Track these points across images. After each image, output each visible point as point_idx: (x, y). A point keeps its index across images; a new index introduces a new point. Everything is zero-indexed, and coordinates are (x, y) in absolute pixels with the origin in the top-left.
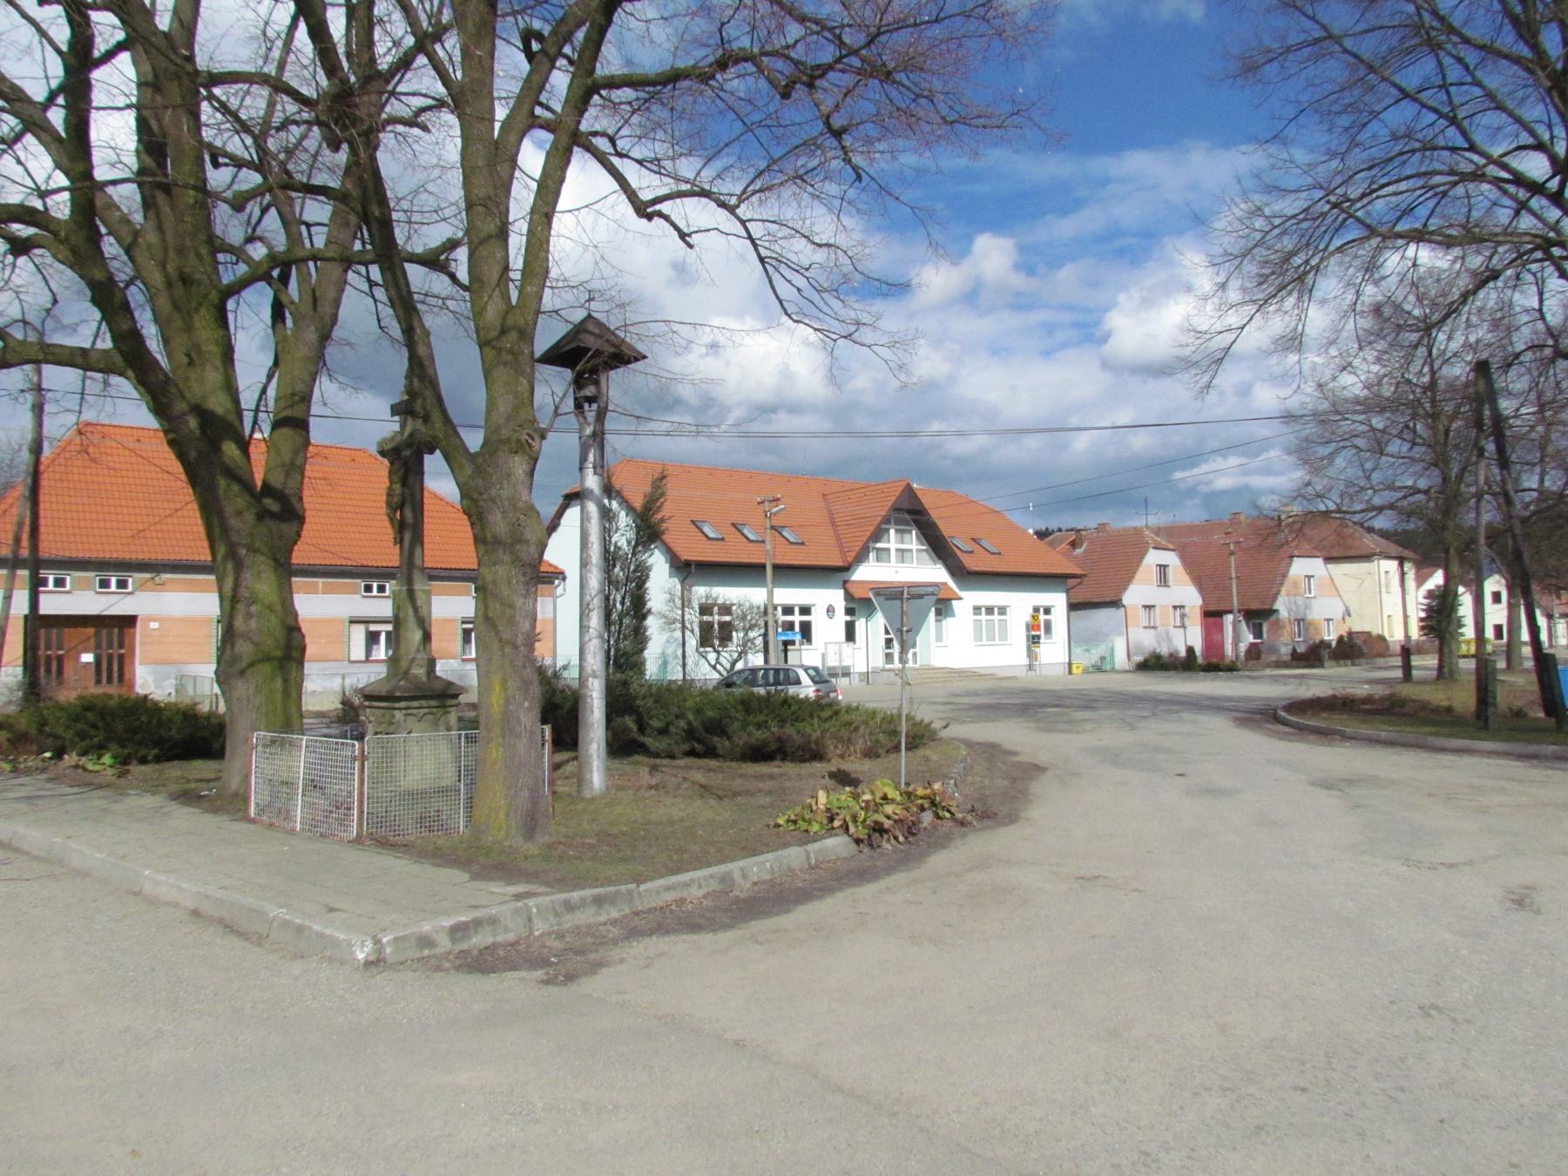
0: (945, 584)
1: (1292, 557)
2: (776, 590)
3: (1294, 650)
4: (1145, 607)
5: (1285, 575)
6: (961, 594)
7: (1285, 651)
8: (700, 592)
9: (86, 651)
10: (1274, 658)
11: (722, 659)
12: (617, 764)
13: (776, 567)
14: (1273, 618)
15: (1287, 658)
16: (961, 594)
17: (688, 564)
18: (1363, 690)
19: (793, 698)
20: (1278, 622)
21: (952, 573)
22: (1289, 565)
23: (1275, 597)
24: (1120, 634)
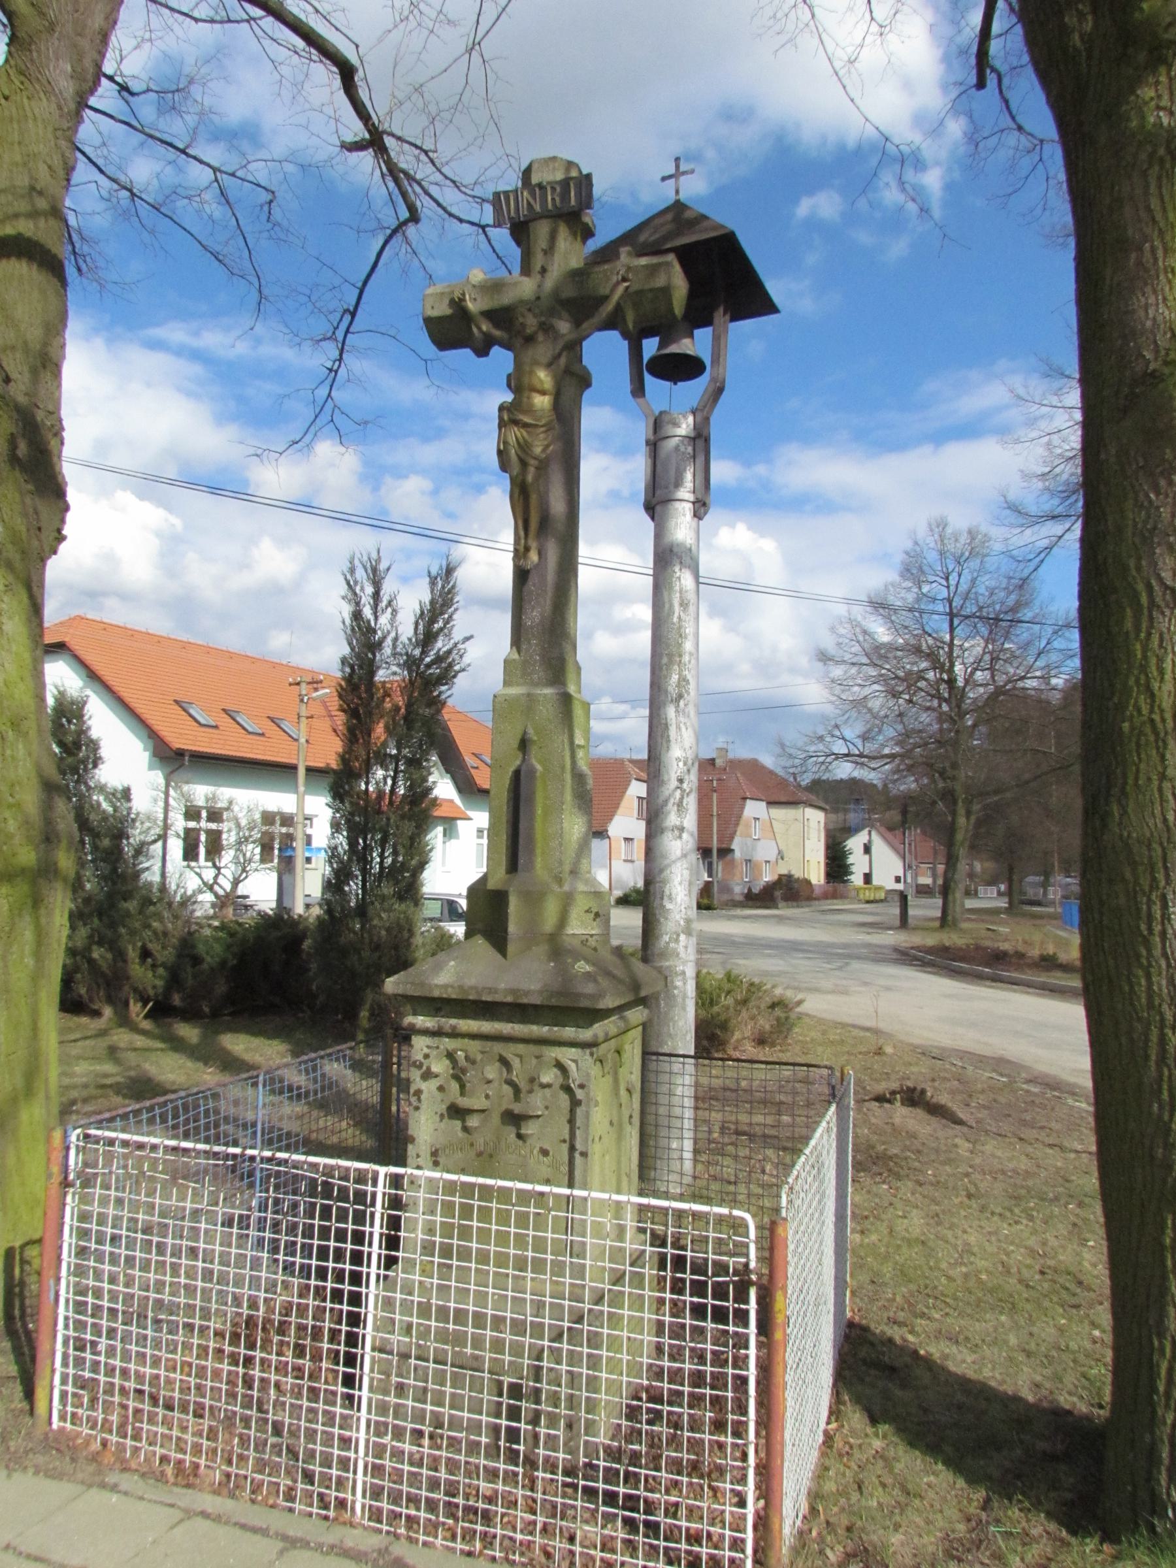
0: (452, 801)
1: (745, 799)
2: (307, 797)
3: (750, 890)
4: (626, 839)
5: (740, 816)
6: (470, 813)
7: (738, 890)
8: (200, 792)
9: (183, 1000)
10: (725, 897)
11: (221, 880)
12: (63, 1015)
13: (309, 770)
14: (729, 857)
15: (740, 898)
16: (470, 813)
17: (180, 753)
18: (1059, 974)
19: (258, 927)
20: (733, 860)
21: (460, 790)
22: (742, 808)
23: (732, 838)
24: (603, 866)
